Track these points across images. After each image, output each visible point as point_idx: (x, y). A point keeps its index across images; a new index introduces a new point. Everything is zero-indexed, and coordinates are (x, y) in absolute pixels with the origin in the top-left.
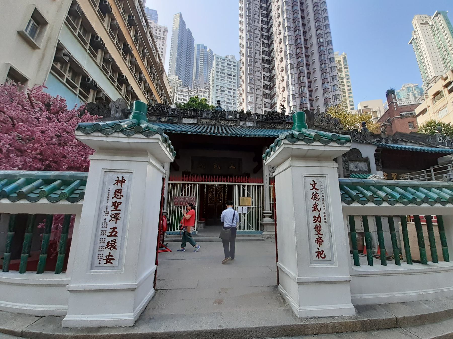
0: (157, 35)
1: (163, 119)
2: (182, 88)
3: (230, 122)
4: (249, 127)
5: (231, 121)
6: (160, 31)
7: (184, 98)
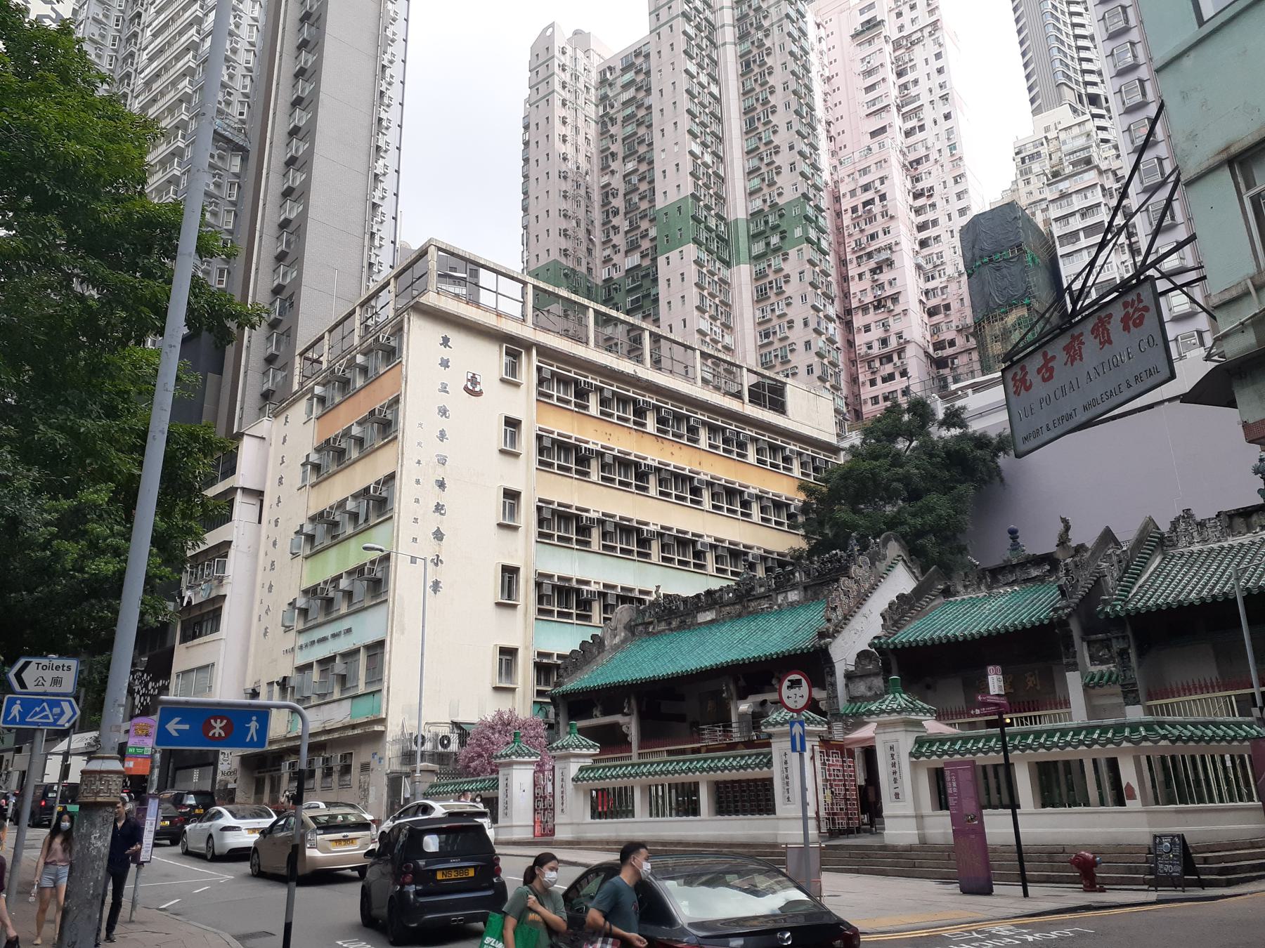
1: (674, 624)
2: (1064, 186)
3: (763, 601)
4: (792, 604)
5: (764, 597)
6: (913, 7)
7: (1090, 221)
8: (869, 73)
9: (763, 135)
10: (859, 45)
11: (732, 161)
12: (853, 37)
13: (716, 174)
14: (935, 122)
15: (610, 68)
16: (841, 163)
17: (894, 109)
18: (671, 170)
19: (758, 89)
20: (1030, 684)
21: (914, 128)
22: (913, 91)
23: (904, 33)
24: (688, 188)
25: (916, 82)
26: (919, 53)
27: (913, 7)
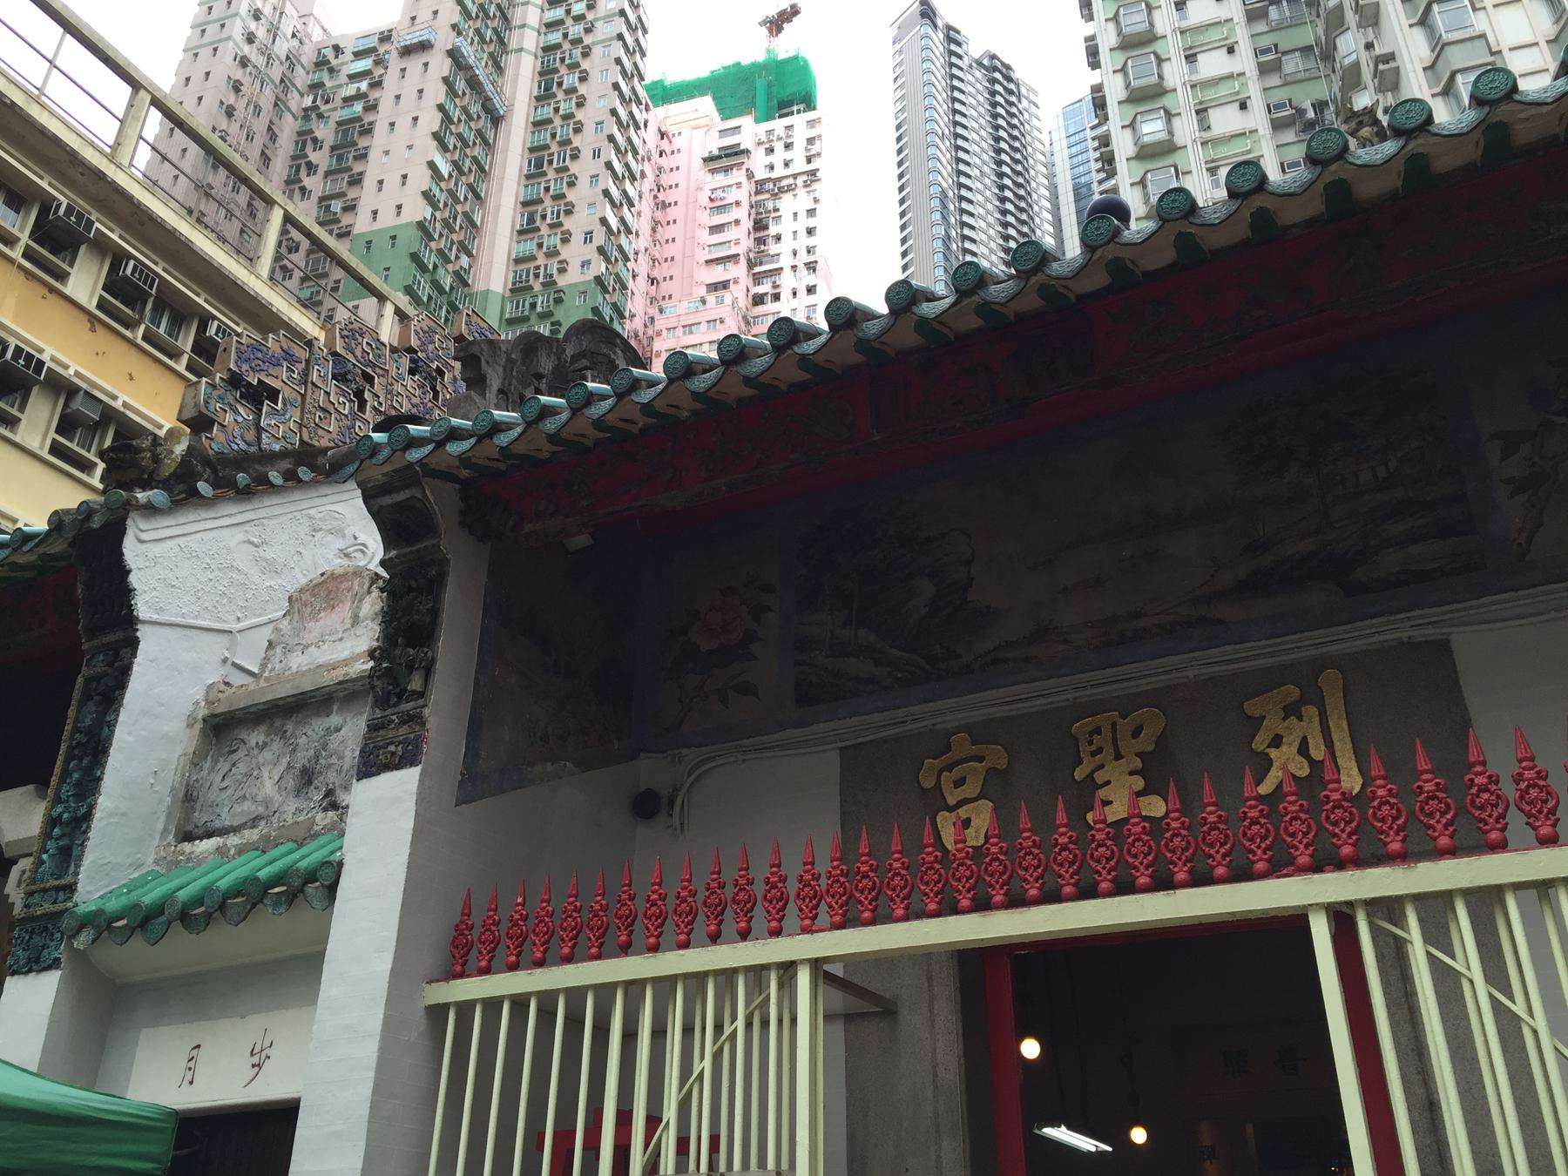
0: (779, 171)
6: (788, 146)
8: (722, 209)
9: (552, 184)
10: (713, 171)
11: (497, 209)
12: (705, 160)
13: (468, 217)
14: (795, 294)
15: (337, 49)
16: (661, 311)
17: (743, 262)
18: (392, 181)
19: (557, 122)
20: (1286, 763)
21: (766, 294)
22: (773, 248)
23: (774, 175)
24: (418, 210)
25: (778, 238)
26: (787, 204)
27: (788, 146)
